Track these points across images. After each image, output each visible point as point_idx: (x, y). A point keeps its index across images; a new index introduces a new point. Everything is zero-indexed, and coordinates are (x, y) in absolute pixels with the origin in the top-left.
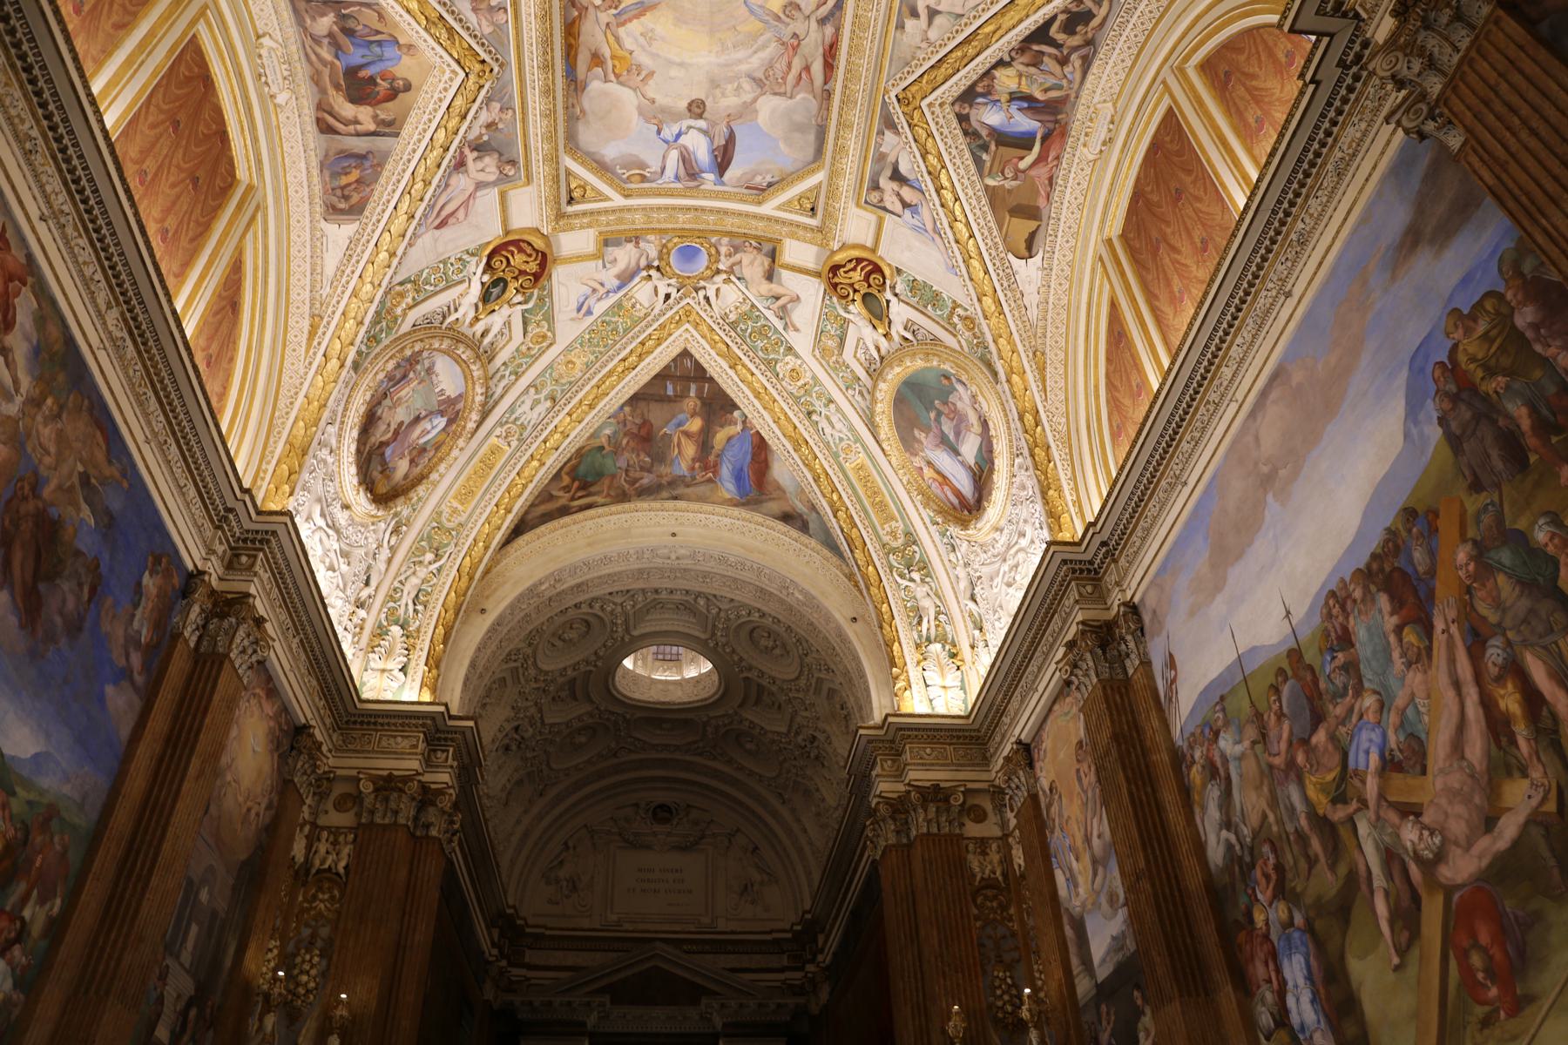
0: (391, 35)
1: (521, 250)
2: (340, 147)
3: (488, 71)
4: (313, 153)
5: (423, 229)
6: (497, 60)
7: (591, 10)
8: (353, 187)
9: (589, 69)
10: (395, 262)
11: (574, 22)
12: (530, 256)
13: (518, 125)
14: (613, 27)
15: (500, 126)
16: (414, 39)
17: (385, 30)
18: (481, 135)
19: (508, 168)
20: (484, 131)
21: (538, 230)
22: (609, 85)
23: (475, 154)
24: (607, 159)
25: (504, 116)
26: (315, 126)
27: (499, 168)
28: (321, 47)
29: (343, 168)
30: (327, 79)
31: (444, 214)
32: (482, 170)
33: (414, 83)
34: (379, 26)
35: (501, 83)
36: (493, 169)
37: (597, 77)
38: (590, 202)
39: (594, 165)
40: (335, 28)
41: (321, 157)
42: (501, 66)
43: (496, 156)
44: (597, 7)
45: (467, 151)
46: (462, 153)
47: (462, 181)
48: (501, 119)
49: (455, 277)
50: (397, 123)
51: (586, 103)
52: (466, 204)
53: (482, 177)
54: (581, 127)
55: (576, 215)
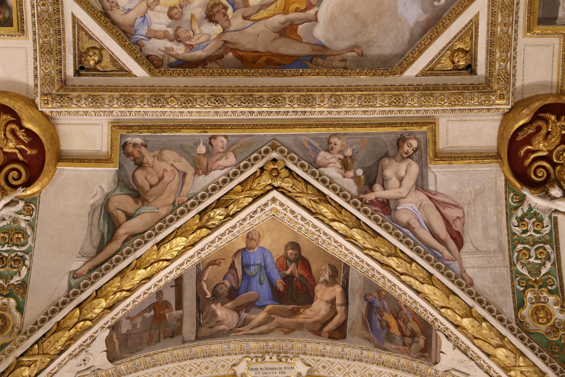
0: (236, 254)
1: (528, 140)
2: (359, 325)
3: (271, 166)
4: (365, 353)
5: (455, 265)
6: (267, 152)
7: (227, 37)
8: (402, 324)
9: (300, 40)
10: (478, 309)
11: (240, 58)
12: (539, 129)
13: (350, 130)
14: (248, 12)
15: (349, 153)
16: (241, 231)
17: (230, 261)
18: (356, 178)
19: (406, 148)
20: (351, 174)
21: (505, 114)
22: (320, 17)
23: (377, 187)
24: (423, 18)
25: (338, 148)
26: (338, 342)
27: (403, 159)
28: (251, 320)
29: (382, 327)
30: (286, 320)
31: (443, 233)
32: (401, 180)
33: (289, 238)
34: (225, 267)
35: (295, 149)
36: (403, 166)
37: (310, 31)
38: (476, 44)
39: (428, 35)
40: (229, 304)
41: (371, 346)
42: (274, 148)
43: (386, 161)
44: (225, 30)
45: (370, 197)
46: (371, 203)
47: (408, 206)
48: (340, 152)
49: (547, 230)
50: (333, 263)
51: (343, 44)
52: (439, 205)
53: (409, 182)
54: (374, 51)
55: (490, 64)
